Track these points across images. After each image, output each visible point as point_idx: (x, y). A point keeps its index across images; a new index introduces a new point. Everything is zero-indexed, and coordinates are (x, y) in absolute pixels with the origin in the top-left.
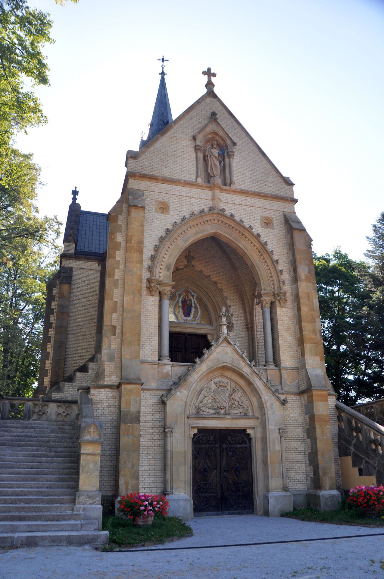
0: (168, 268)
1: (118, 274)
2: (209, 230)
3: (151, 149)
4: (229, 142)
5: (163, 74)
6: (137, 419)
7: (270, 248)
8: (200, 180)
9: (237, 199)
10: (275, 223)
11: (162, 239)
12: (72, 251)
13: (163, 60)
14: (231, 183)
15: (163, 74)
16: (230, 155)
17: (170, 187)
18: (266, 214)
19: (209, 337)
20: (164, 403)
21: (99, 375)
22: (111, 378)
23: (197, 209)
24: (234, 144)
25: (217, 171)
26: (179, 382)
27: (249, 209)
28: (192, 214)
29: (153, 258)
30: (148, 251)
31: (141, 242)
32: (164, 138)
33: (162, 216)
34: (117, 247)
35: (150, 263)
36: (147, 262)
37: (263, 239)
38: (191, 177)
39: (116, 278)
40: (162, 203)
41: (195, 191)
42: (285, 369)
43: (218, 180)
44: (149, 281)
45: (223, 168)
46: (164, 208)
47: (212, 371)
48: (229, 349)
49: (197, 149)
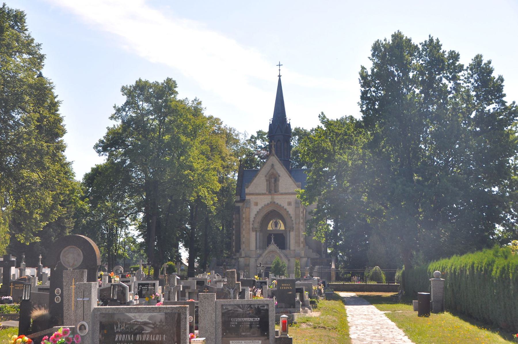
0: (258, 223)
1: (244, 227)
2: (271, 209)
3: (252, 183)
4: (277, 176)
5: (280, 76)
6: (248, 265)
7: (290, 213)
8: (267, 193)
9: (280, 197)
10: (292, 203)
11: (256, 215)
12: (239, 199)
13: (280, 65)
14: (278, 191)
15: (280, 76)
16: (279, 181)
17: (259, 196)
18: (289, 200)
19: (284, 234)
20: (256, 261)
21: (241, 255)
22: (243, 255)
23: (266, 203)
24: (279, 176)
25: (273, 188)
26: (260, 255)
27: (283, 200)
28: (265, 205)
29: (253, 221)
30: (252, 219)
31: (249, 218)
32: (256, 178)
33: (256, 207)
34: (243, 219)
35: (253, 222)
36: (251, 222)
37: (288, 210)
38: (264, 192)
39: (244, 228)
40: (256, 202)
41: (266, 196)
42: (291, 250)
43: (273, 192)
44: (253, 228)
45: (275, 186)
46: (256, 204)
47: (269, 252)
48: (274, 246)
49: (267, 181)
